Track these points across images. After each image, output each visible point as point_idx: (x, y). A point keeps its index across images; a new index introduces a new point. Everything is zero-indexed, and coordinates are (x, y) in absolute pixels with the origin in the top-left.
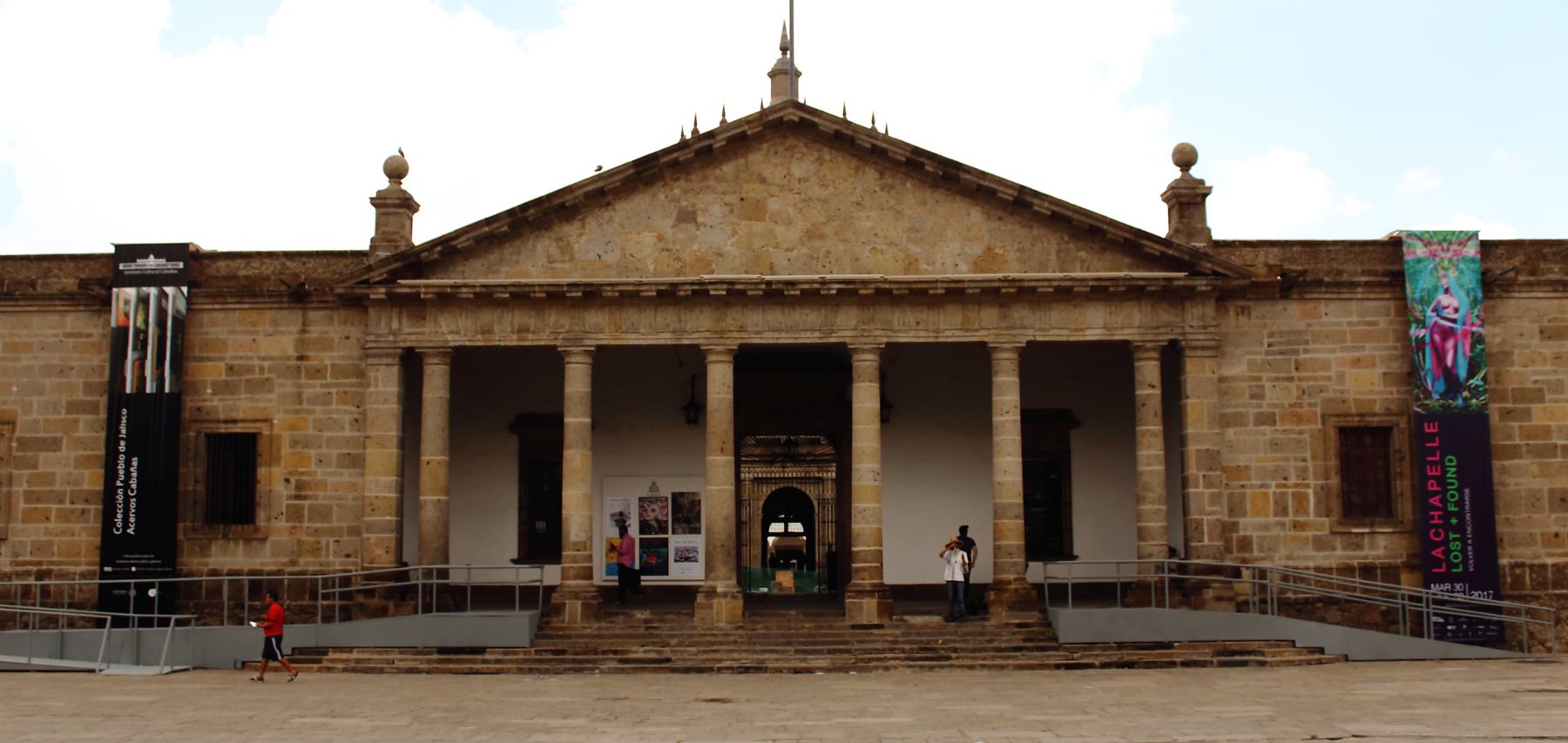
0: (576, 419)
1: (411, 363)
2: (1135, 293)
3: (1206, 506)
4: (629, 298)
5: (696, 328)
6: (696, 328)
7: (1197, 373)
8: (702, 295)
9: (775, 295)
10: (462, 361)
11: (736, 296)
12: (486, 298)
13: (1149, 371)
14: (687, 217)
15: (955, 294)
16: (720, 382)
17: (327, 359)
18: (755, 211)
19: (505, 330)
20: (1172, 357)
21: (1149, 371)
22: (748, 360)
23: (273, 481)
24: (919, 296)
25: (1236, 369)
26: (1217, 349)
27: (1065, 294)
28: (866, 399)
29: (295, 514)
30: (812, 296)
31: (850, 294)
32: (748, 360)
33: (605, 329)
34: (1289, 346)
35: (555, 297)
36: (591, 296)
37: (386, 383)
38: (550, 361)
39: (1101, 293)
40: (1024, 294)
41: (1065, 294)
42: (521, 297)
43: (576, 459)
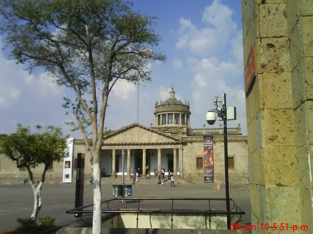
4: (119, 145)
7: (180, 152)
9: (134, 144)
15: (153, 144)
20: (177, 150)
21: (175, 152)
22: (131, 151)
24: (149, 144)
27: (164, 144)
30: (137, 144)
31: (141, 144)
34: (191, 149)
35: (111, 145)
36: (115, 145)
39: (168, 144)
40: (160, 144)
41: (164, 144)
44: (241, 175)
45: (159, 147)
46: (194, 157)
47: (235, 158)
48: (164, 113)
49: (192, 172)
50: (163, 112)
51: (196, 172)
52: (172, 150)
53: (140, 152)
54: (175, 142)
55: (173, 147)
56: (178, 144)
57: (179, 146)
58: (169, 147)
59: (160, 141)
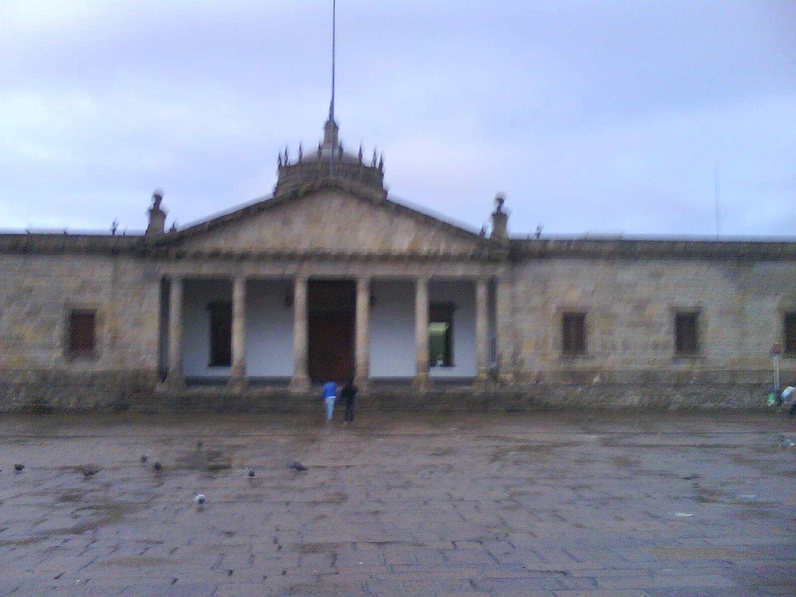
0: (238, 307)
1: (165, 285)
2: (474, 258)
3: (505, 349)
4: (262, 258)
5: (290, 269)
6: (290, 269)
8: (292, 257)
11: (306, 257)
15: (399, 259)
16: (300, 293)
19: (207, 270)
20: (492, 286)
21: (481, 292)
22: (314, 285)
23: (103, 333)
24: (386, 258)
25: (521, 288)
26: (512, 281)
27: (446, 258)
28: (362, 301)
30: (339, 258)
31: (354, 258)
32: (314, 285)
33: (250, 270)
35: (229, 256)
37: (155, 291)
38: (226, 284)
39: (461, 258)
42: (215, 255)
43: (238, 325)
44: (725, 380)
45: (422, 274)
46: (553, 311)
47: (700, 318)
51: (562, 366)
52: (468, 286)
53: (348, 287)
55: (473, 271)
56: (492, 260)
57: (501, 271)
58: (459, 271)
59: (425, 248)
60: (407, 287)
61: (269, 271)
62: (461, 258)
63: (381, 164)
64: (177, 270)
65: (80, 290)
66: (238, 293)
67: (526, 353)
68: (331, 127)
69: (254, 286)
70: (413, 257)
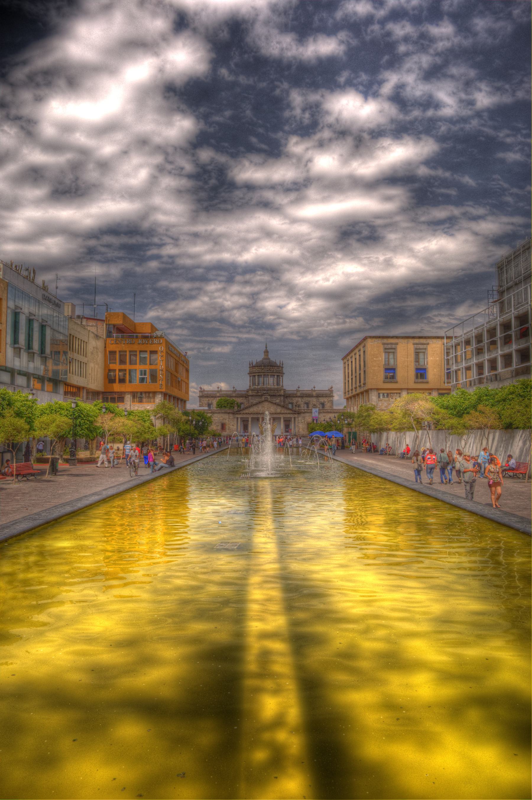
1: (237, 418)
7: (297, 419)
8: (259, 414)
10: (241, 418)
12: (243, 414)
13: (293, 419)
14: (258, 407)
15: (278, 413)
17: (231, 418)
18: (264, 407)
19: (245, 416)
20: (295, 418)
21: (293, 419)
23: (227, 427)
24: (276, 413)
25: (300, 419)
27: (286, 413)
29: (229, 430)
34: (304, 417)
36: (251, 414)
37: (236, 420)
38: (248, 418)
39: (289, 413)
41: (286, 413)
45: (281, 416)
48: (260, 374)
49: (304, 433)
50: (259, 373)
52: (291, 418)
54: (293, 412)
55: (292, 416)
57: (296, 416)
58: (289, 416)
60: (280, 418)
61: (255, 416)
62: (289, 413)
63: (283, 364)
64: (239, 416)
65: (223, 420)
66: (250, 420)
67: (301, 430)
68: (266, 352)
69: (252, 418)
70: (280, 413)
